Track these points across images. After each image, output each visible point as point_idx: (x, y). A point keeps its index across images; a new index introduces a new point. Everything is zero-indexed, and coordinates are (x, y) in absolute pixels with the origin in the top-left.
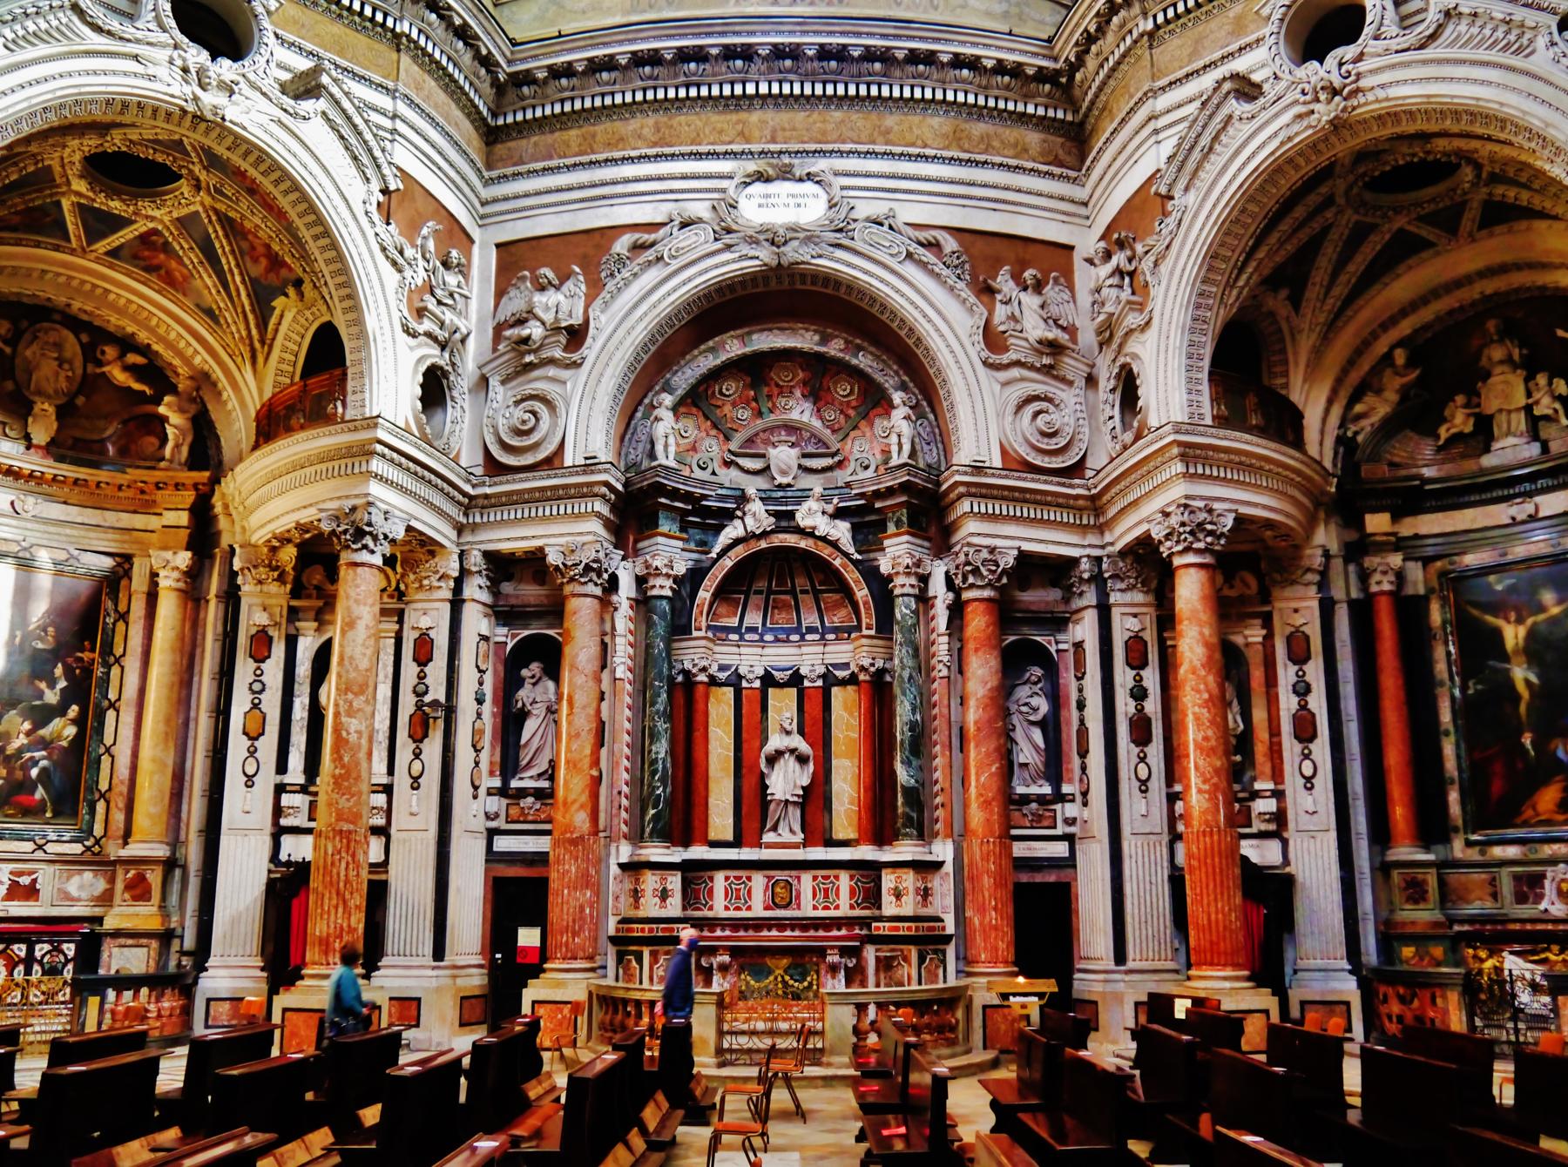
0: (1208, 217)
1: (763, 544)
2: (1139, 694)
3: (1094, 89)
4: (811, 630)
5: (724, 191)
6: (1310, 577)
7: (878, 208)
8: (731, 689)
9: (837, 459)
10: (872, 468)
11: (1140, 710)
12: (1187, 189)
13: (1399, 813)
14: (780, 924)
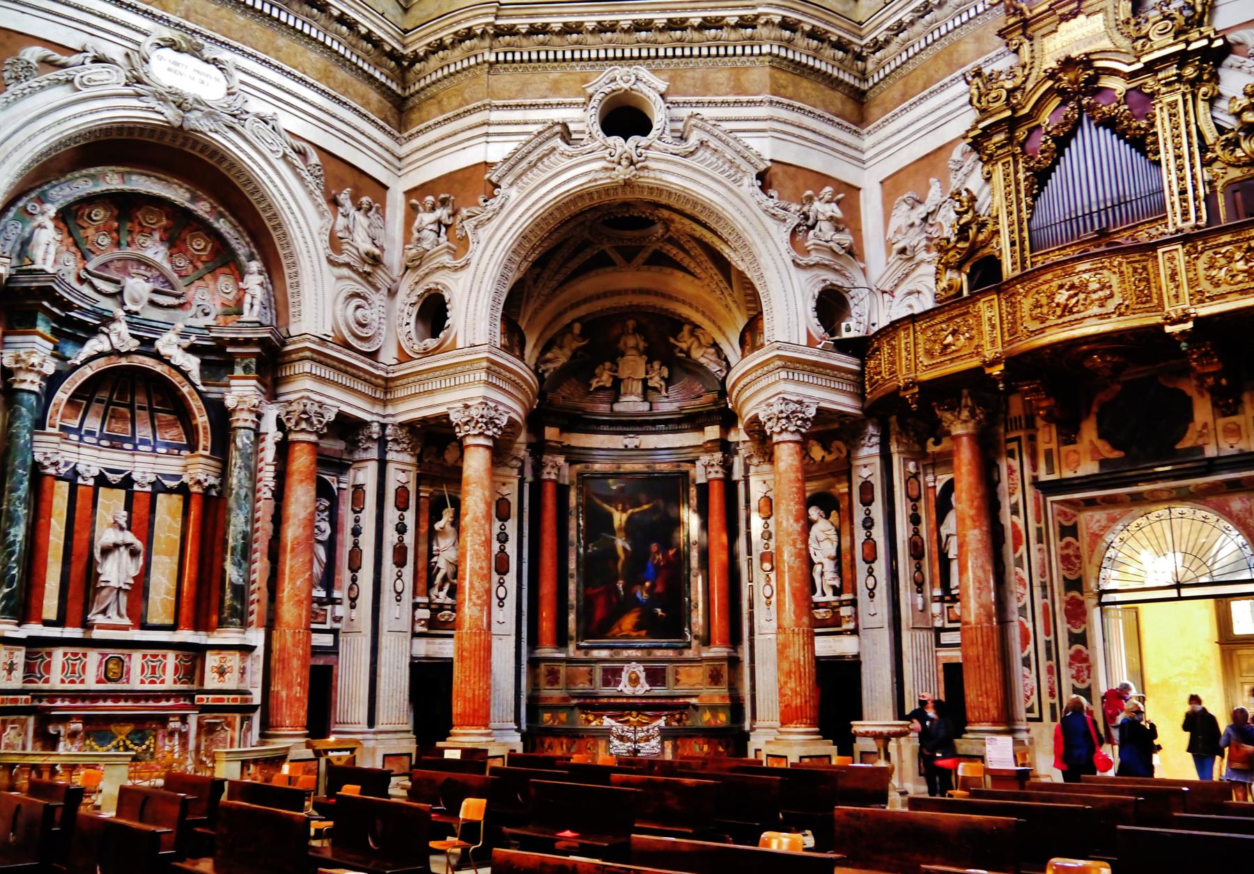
0: (527, 210)
1: (124, 362)
2: (401, 529)
3: (428, 81)
4: (144, 442)
5: (138, 44)
6: (514, 462)
7: (267, 110)
8: (67, 484)
9: (182, 301)
10: (212, 316)
11: (401, 541)
12: (511, 185)
13: (546, 626)
14: (116, 696)
